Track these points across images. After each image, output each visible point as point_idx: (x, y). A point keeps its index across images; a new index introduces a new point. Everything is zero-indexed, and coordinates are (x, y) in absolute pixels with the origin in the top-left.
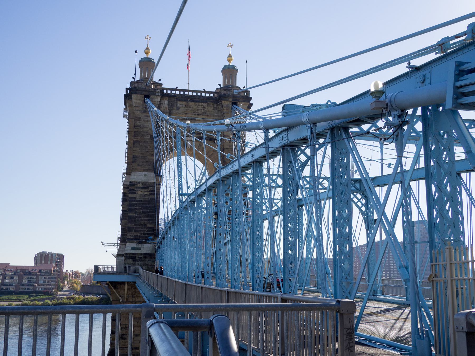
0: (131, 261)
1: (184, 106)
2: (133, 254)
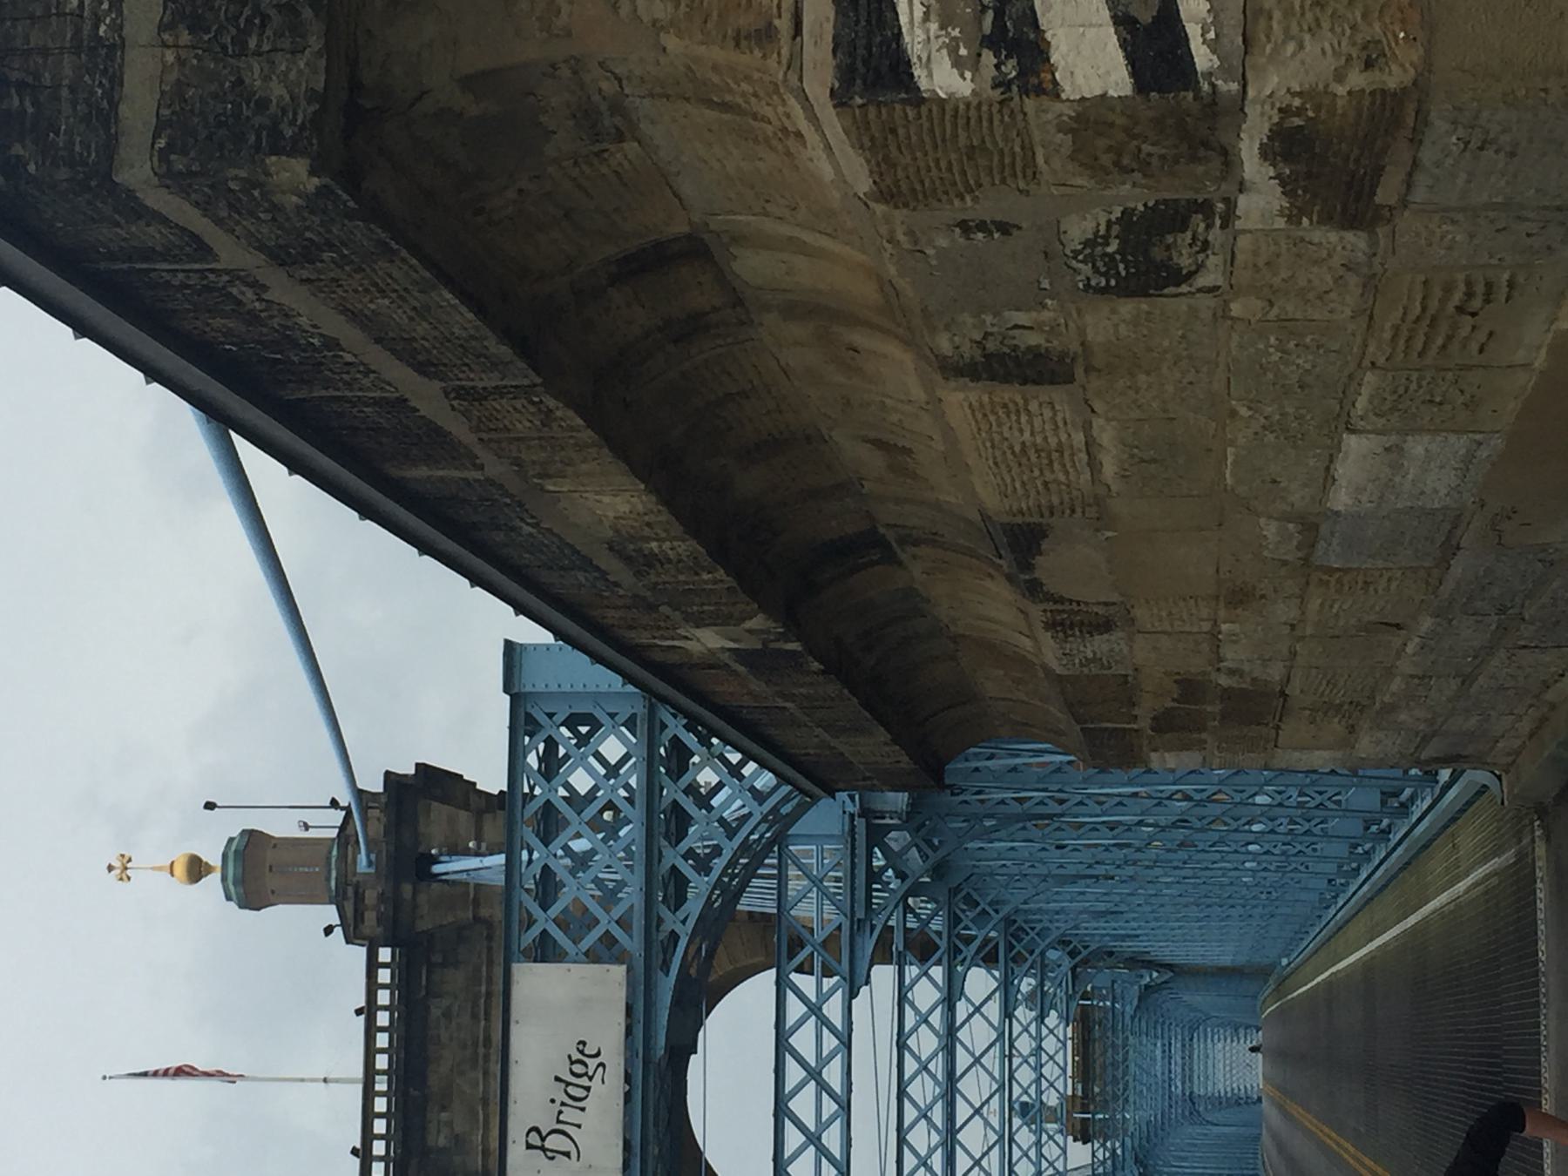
1: (444, 1116)
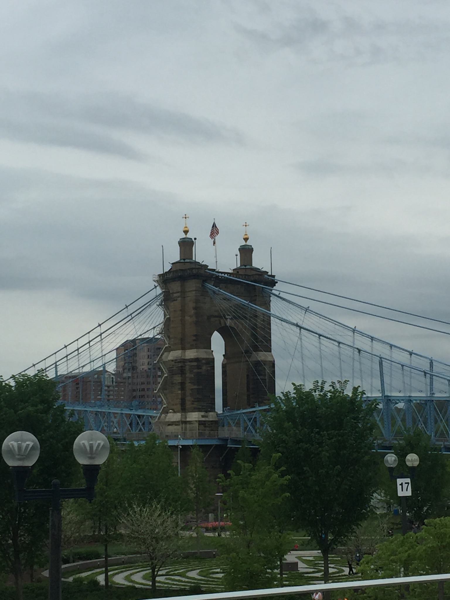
0: (202, 427)
2: (204, 421)
